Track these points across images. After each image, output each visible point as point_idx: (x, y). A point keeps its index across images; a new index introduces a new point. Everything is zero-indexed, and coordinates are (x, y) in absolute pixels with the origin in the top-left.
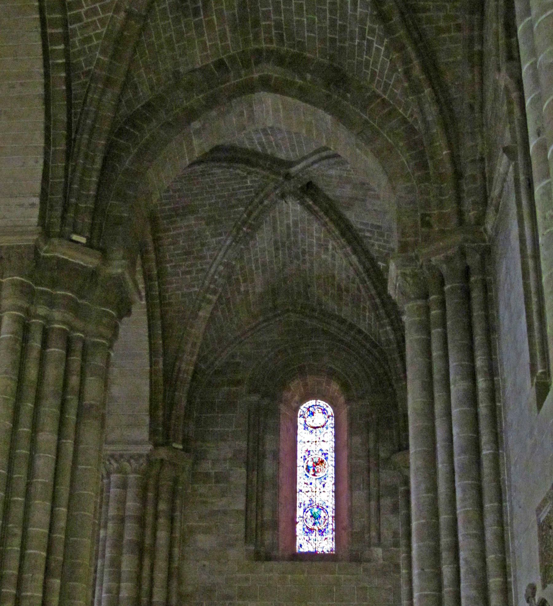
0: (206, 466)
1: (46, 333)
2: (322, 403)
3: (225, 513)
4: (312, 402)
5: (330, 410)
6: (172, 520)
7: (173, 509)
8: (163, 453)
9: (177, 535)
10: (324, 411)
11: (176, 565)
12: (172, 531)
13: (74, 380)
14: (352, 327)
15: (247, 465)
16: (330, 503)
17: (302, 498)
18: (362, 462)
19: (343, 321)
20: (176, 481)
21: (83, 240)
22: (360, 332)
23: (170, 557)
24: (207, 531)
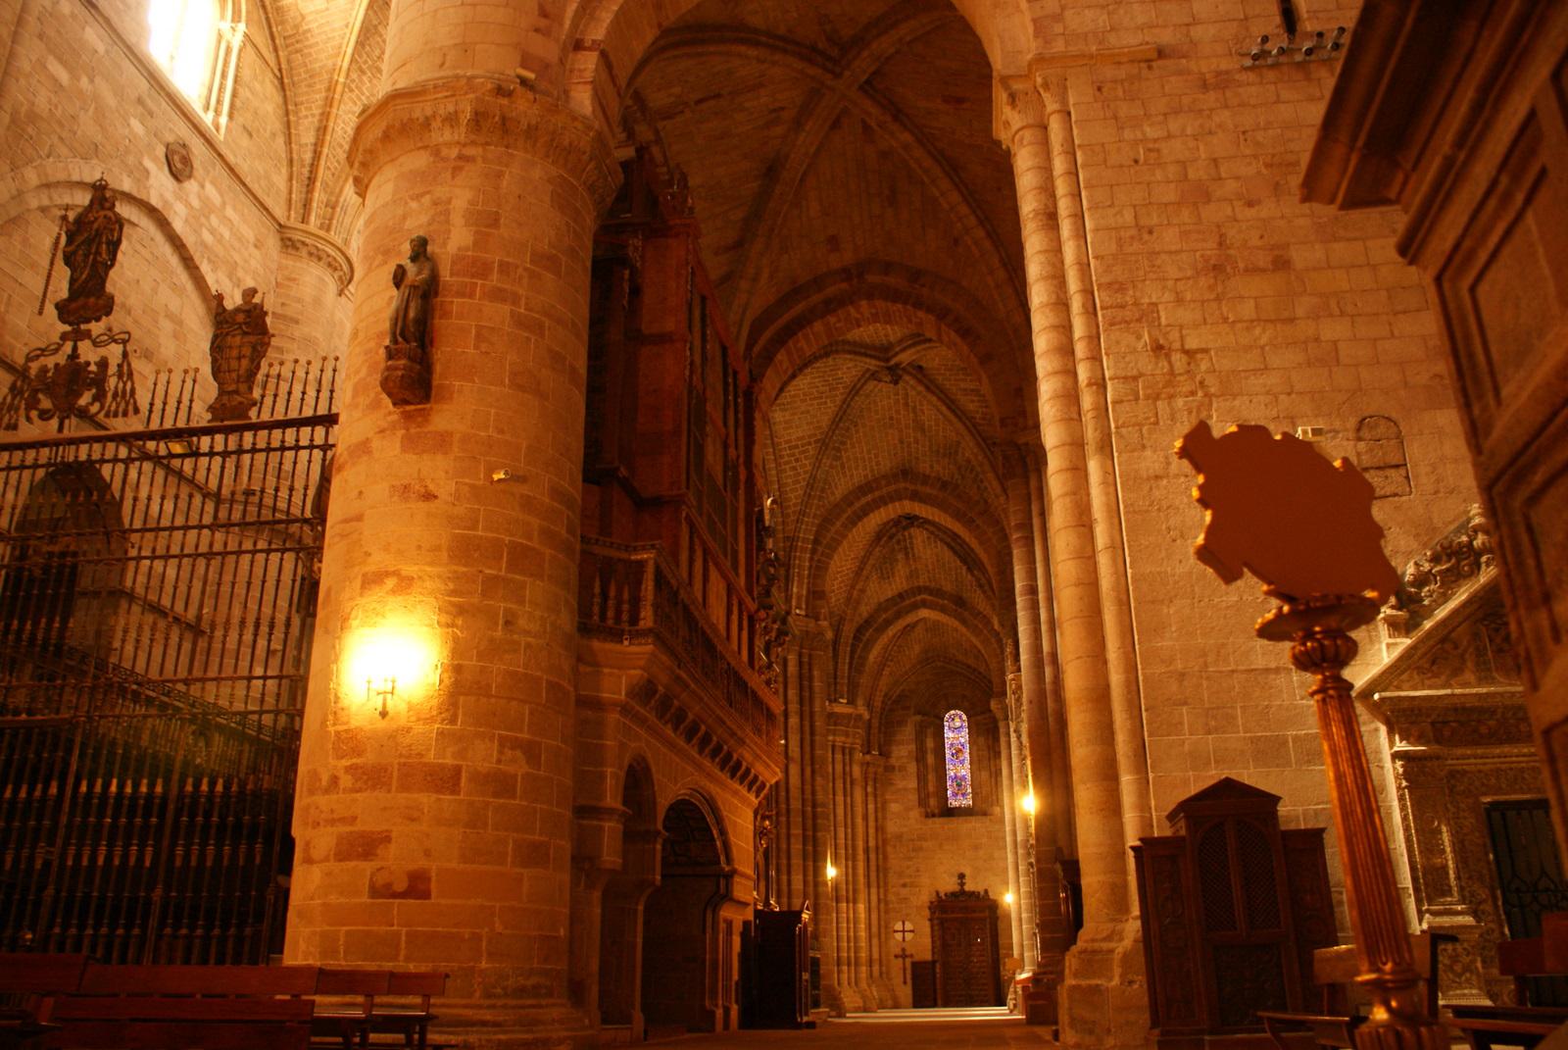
0: (893, 761)
1: (833, 747)
2: (959, 712)
3: (905, 789)
4: (952, 712)
5: (964, 717)
6: (875, 796)
7: (875, 789)
8: (868, 757)
9: (879, 805)
10: (960, 717)
11: (880, 821)
12: (876, 803)
13: (847, 769)
14: (975, 670)
15: (917, 761)
16: (969, 777)
17: (951, 773)
18: (985, 753)
19: (969, 667)
20: (876, 773)
21: (845, 701)
22: (980, 673)
23: (876, 820)
24: (896, 801)
